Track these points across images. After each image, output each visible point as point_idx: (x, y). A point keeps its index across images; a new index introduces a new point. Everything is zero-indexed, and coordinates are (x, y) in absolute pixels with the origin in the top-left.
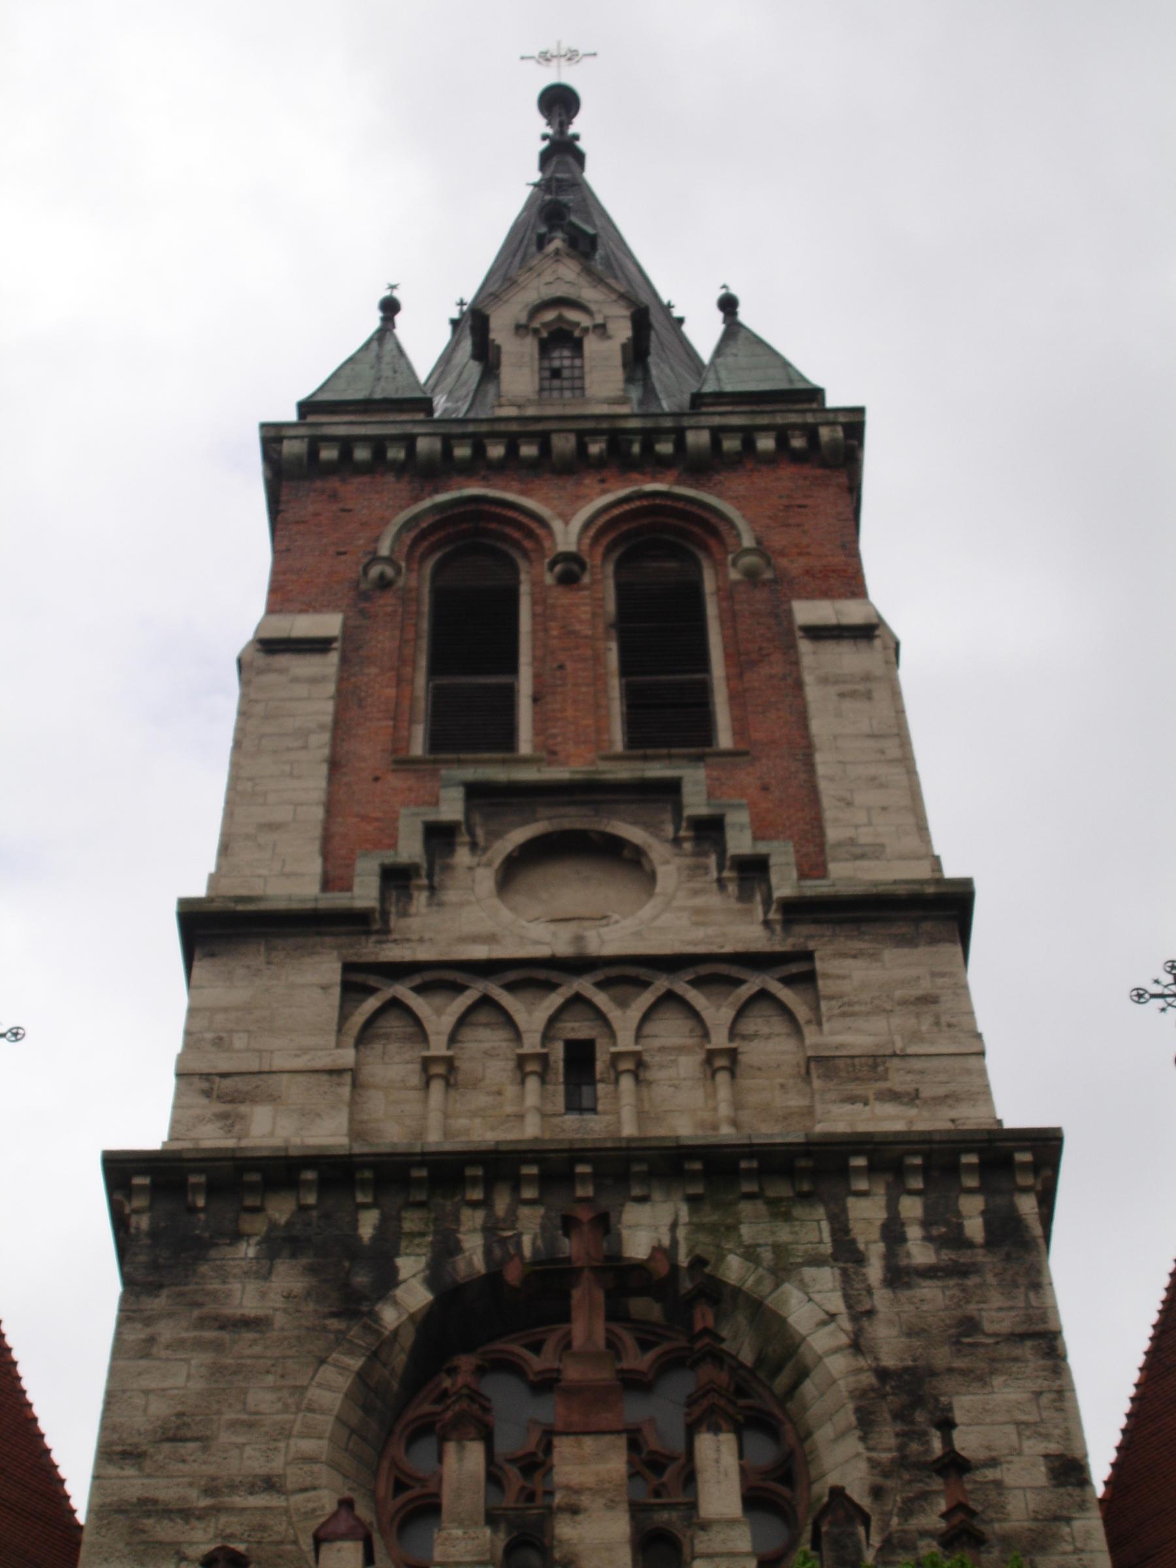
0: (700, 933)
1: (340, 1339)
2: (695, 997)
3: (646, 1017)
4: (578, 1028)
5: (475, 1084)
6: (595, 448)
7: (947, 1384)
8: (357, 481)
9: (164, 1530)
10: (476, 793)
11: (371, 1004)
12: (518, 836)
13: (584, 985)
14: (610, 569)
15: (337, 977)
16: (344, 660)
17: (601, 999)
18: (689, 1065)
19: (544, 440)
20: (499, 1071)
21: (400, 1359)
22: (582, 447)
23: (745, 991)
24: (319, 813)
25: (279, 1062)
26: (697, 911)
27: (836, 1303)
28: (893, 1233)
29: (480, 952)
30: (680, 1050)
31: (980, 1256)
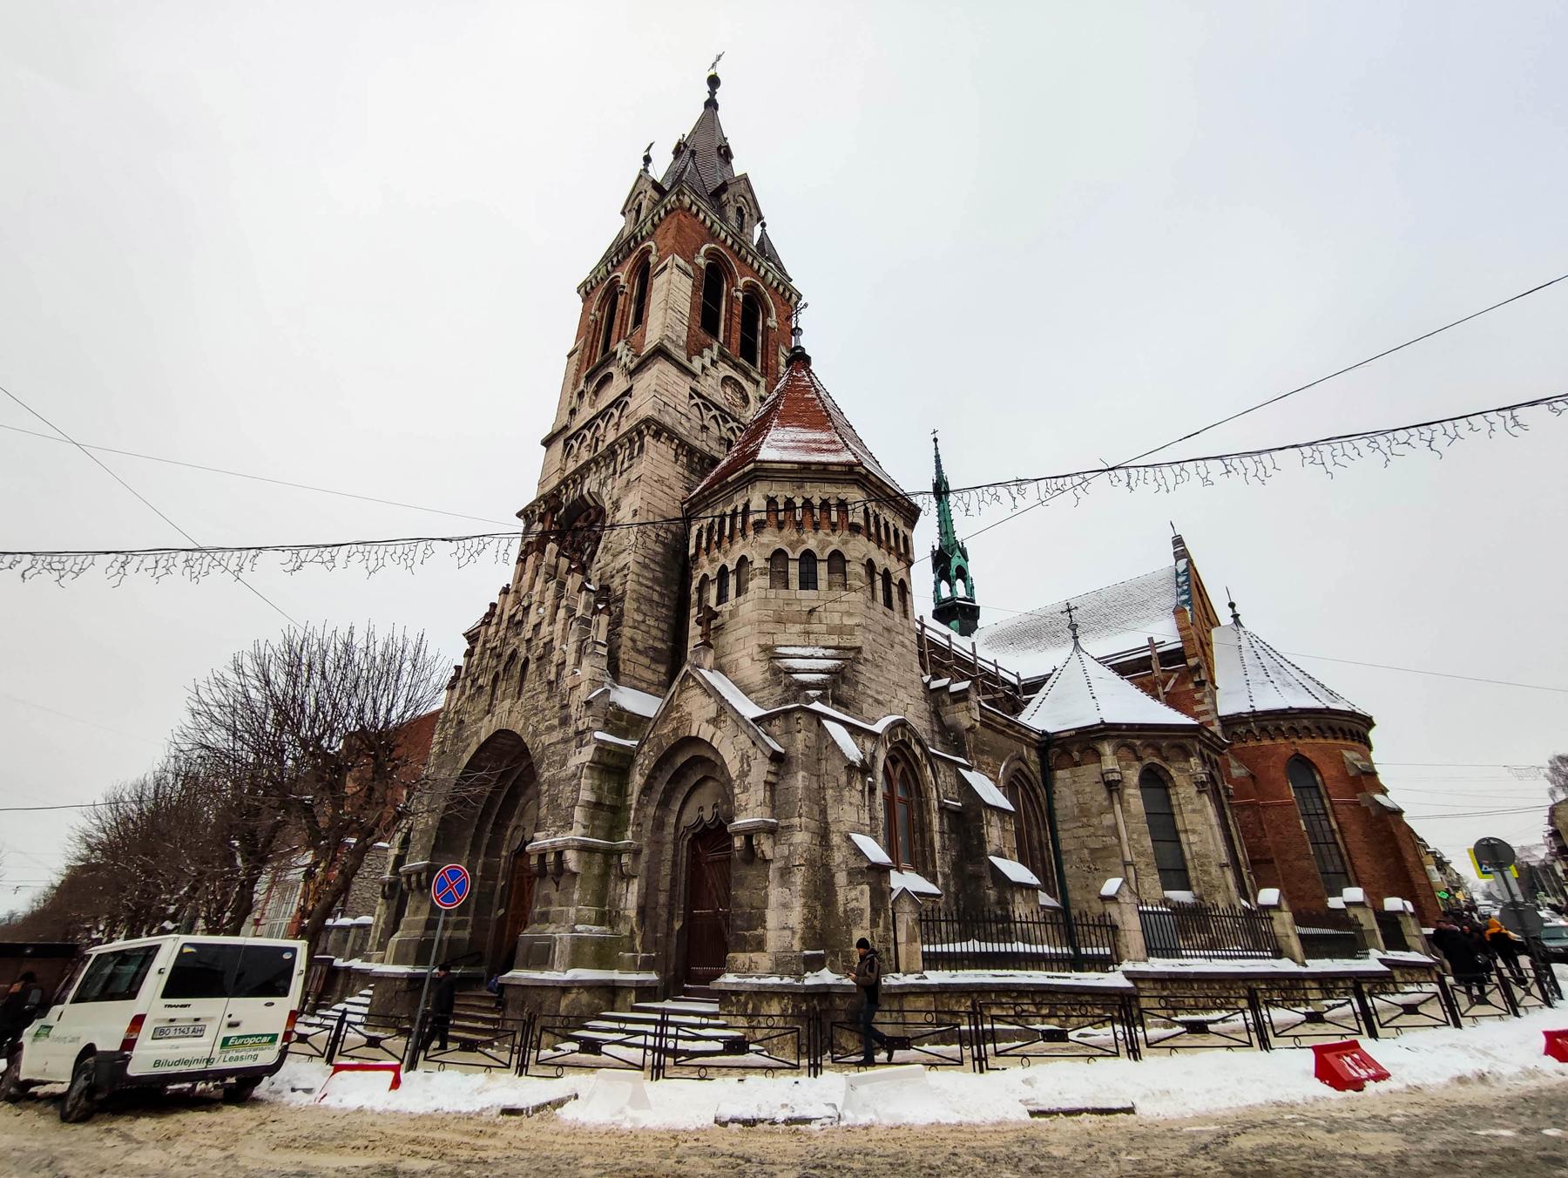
3: (608, 422)
27: (609, 488)
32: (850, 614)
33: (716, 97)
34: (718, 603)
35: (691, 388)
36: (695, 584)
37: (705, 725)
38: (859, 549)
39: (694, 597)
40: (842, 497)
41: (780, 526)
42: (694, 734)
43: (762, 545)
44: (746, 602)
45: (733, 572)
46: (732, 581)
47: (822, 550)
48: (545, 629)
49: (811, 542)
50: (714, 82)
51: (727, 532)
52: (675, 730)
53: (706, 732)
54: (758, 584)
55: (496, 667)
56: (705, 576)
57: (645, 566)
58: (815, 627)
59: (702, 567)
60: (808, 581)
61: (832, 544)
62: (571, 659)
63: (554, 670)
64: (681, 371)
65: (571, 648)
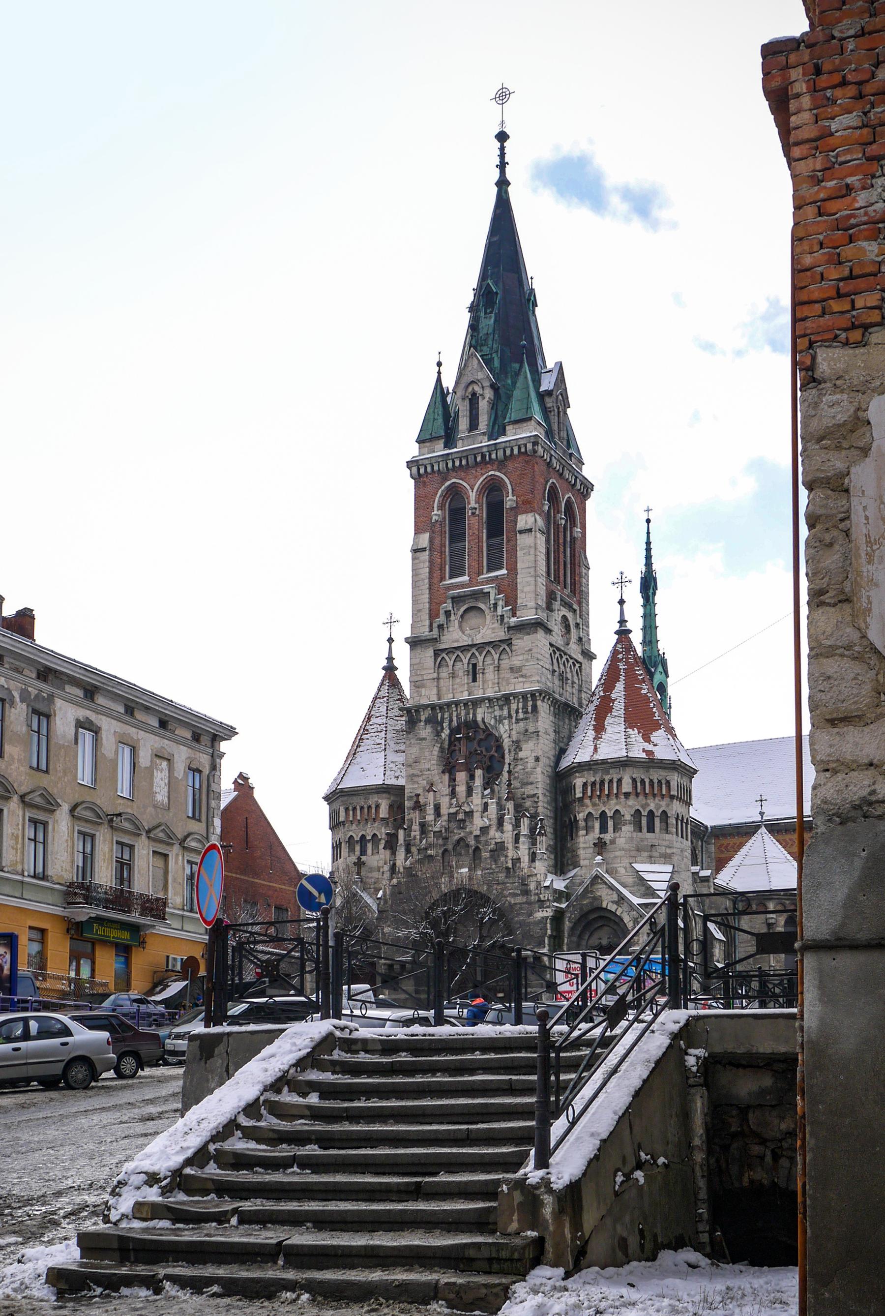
0: (493, 635)
1: (437, 741)
2: (493, 651)
4: (473, 661)
5: (457, 676)
6: (479, 459)
7: (521, 743)
8: (429, 476)
9: (416, 779)
10: (453, 598)
11: (439, 659)
12: (462, 609)
13: (474, 650)
14: (485, 499)
15: (433, 654)
16: (430, 550)
17: (477, 654)
18: (492, 667)
19: (467, 457)
20: (461, 673)
21: (447, 743)
22: (475, 458)
23: (501, 648)
24: (427, 605)
25: (425, 678)
26: (493, 629)
27: (507, 727)
28: (517, 712)
29: (456, 645)
30: (491, 664)
31: (530, 715)
32: (670, 847)
33: (507, 176)
34: (600, 833)
35: (551, 645)
36: (581, 816)
37: (610, 904)
38: (676, 807)
39: (582, 824)
40: (668, 778)
41: (637, 795)
42: (604, 906)
43: (629, 806)
44: (620, 837)
45: (611, 817)
46: (610, 823)
47: (657, 810)
48: (493, 832)
49: (652, 806)
50: (502, 137)
51: (607, 792)
52: (591, 903)
53: (612, 907)
54: (627, 829)
55: (444, 845)
56: (590, 813)
57: (545, 795)
58: (655, 854)
59: (587, 806)
60: (651, 829)
61: (661, 806)
62: (525, 859)
63: (510, 862)
64: (546, 633)
65: (523, 852)
